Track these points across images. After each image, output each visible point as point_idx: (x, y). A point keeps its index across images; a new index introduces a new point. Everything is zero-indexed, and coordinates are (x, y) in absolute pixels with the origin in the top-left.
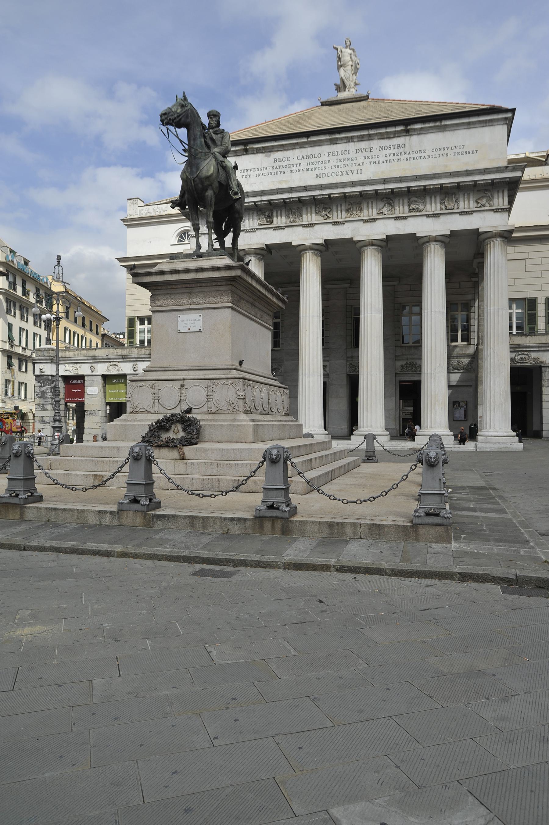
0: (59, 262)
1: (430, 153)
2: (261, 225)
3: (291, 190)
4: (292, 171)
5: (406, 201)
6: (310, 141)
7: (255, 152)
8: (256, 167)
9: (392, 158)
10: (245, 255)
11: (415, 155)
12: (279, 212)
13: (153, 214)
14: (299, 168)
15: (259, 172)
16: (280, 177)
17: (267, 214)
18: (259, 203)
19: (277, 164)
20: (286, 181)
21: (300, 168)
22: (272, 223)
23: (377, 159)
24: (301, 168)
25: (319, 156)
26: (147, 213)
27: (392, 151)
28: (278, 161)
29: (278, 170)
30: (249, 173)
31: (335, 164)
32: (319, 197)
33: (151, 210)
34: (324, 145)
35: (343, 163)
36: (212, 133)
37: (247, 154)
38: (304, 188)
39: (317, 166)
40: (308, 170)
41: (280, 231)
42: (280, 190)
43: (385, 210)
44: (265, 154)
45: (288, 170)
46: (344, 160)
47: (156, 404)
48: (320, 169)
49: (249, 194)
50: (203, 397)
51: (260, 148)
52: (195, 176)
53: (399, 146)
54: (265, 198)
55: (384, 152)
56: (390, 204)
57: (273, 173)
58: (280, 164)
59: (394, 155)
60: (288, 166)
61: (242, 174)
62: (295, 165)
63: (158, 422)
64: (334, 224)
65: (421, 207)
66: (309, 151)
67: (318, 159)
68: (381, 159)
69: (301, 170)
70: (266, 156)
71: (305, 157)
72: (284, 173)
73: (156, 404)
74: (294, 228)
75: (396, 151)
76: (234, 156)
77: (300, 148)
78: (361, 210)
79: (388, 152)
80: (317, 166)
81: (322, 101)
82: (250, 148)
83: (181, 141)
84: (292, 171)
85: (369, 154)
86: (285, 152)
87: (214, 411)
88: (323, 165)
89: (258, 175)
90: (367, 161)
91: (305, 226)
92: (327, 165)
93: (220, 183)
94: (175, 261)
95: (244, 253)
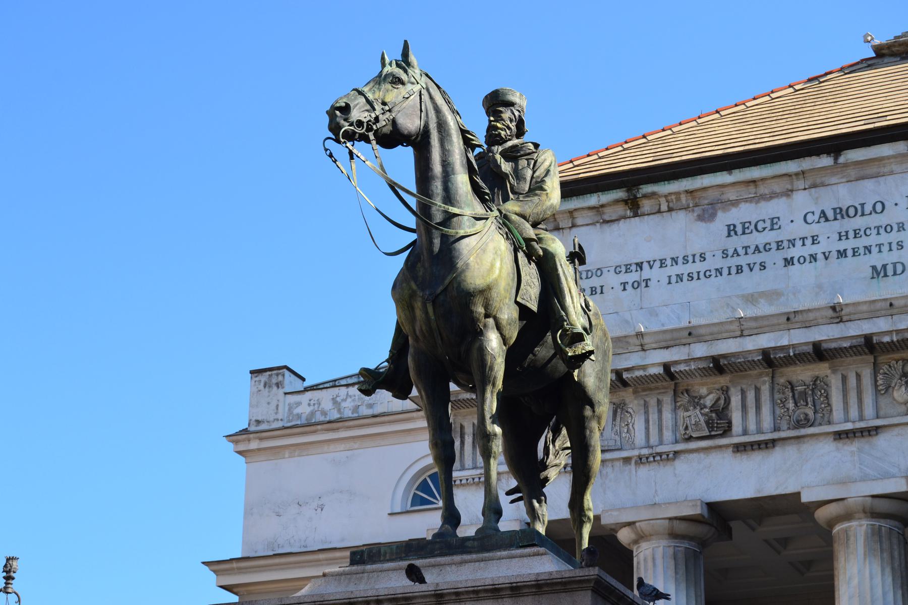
0: (8, 578)
2: (690, 439)
3: (790, 319)
4: (789, 262)
6: (846, 165)
7: (664, 207)
8: (668, 255)
10: (636, 542)
12: (751, 396)
13: (336, 416)
14: (810, 249)
15: (680, 269)
16: (750, 282)
17: (709, 401)
18: (682, 367)
19: (737, 242)
20: (772, 295)
21: (815, 249)
22: (727, 431)
24: (818, 249)
25: (879, 207)
26: (313, 413)
28: (739, 229)
29: (743, 261)
30: (646, 273)
32: (886, 339)
33: (327, 405)
34: (892, 173)
36: (498, 157)
37: (636, 215)
38: (830, 313)
39: (872, 240)
40: (842, 254)
41: (756, 458)
42: (753, 324)
44: (698, 211)
45: (775, 258)
48: (885, 248)
49: (647, 340)
51: (678, 194)
52: (439, 291)
54: (700, 350)
57: (725, 272)
58: (746, 240)
60: (774, 246)
61: (624, 277)
62: (799, 243)
66: (843, 194)
69: (820, 256)
70: (701, 218)
71: (830, 214)
72: (763, 266)
74: (808, 447)
76: (593, 224)
77: (814, 186)
80: (872, 240)
81: (877, 42)
82: (645, 196)
83: (393, 186)
84: (789, 262)
86: (763, 204)
89: (674, 279)
91: (840, 436)
93: (523, 310)
94: (369, 567)
95: (633, 536)
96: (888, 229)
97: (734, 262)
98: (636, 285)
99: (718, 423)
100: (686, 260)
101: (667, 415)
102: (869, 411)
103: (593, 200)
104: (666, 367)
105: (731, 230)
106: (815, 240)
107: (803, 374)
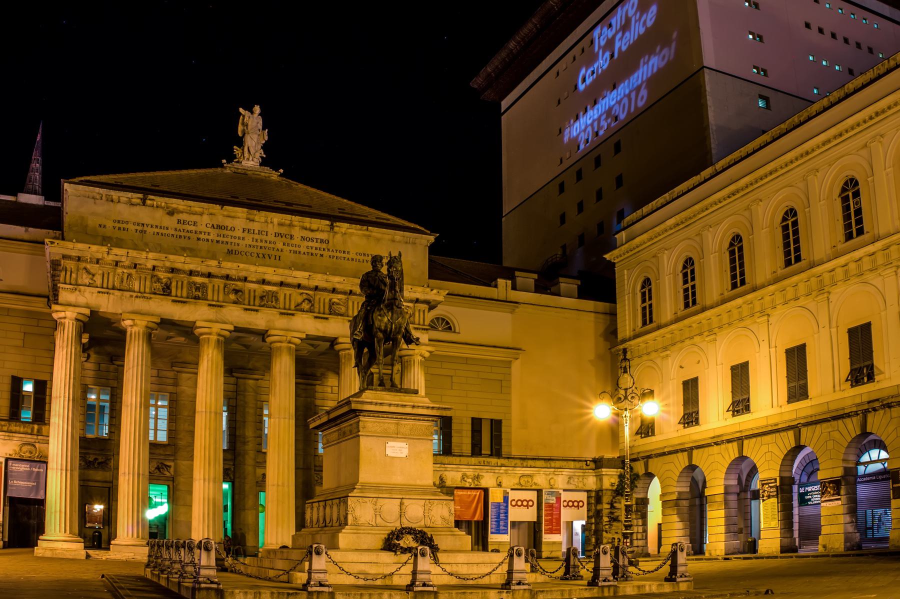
1: (355, 257)
2: (155, 293)
5: (327, 301)
9: (314, 251)
11: (338, 254)
19: (179, 226)
23: (297, 249)
24: (210, 238)
27: (314, 244)
31: (250, 242)
35: (260, 244)
39: (229, 240)
43: (306, 306)
46: (261, 241)
47: (378, 517)
50: (421, 514)
53: (322, 241)
55: (306, 243)
56: (310, 301)
59: (316, 249)
63: (392, 533)
64: (246, 309)
65: (343, 310)
67: (230, 233)
68: (303, 250)
72: (189, 238)
73: (378, 517)
75: (318, 245)
78: (277, 300)
79: (310, 244)
84: (199, 239)
85: (288, 241)
87: (428, 524)
88: (237, 241)
90: (286, 248)
92: (241, 242)
96: (235, 238)
97: (179, 233)
98: (141, 232)
99: (166, 290)
100: (161, 228)
101: (148, 283)
102: (221, 299)
103: (130, 195)
104: (154, 267)
105: (179, 221)
106: (209, 234)
107: (199, 280)
